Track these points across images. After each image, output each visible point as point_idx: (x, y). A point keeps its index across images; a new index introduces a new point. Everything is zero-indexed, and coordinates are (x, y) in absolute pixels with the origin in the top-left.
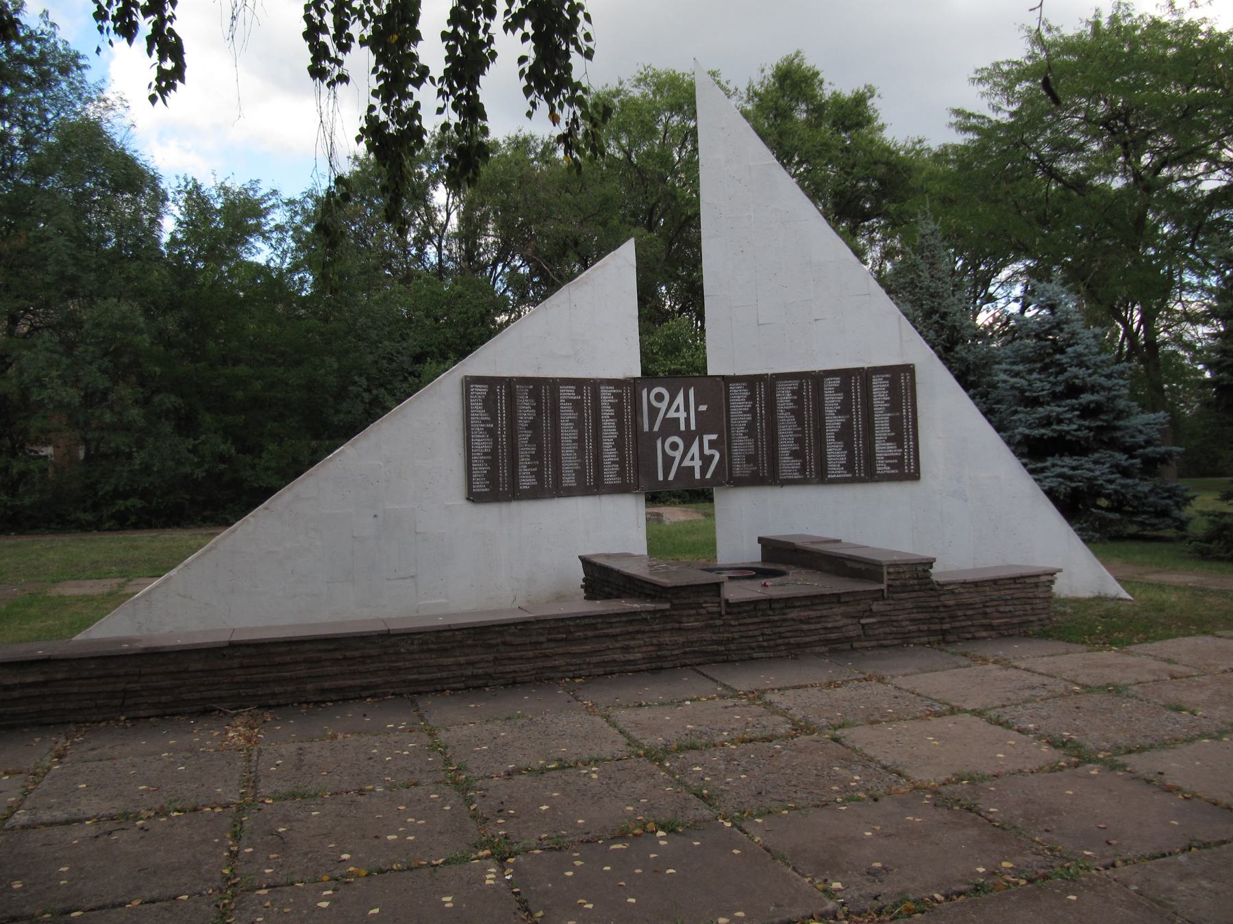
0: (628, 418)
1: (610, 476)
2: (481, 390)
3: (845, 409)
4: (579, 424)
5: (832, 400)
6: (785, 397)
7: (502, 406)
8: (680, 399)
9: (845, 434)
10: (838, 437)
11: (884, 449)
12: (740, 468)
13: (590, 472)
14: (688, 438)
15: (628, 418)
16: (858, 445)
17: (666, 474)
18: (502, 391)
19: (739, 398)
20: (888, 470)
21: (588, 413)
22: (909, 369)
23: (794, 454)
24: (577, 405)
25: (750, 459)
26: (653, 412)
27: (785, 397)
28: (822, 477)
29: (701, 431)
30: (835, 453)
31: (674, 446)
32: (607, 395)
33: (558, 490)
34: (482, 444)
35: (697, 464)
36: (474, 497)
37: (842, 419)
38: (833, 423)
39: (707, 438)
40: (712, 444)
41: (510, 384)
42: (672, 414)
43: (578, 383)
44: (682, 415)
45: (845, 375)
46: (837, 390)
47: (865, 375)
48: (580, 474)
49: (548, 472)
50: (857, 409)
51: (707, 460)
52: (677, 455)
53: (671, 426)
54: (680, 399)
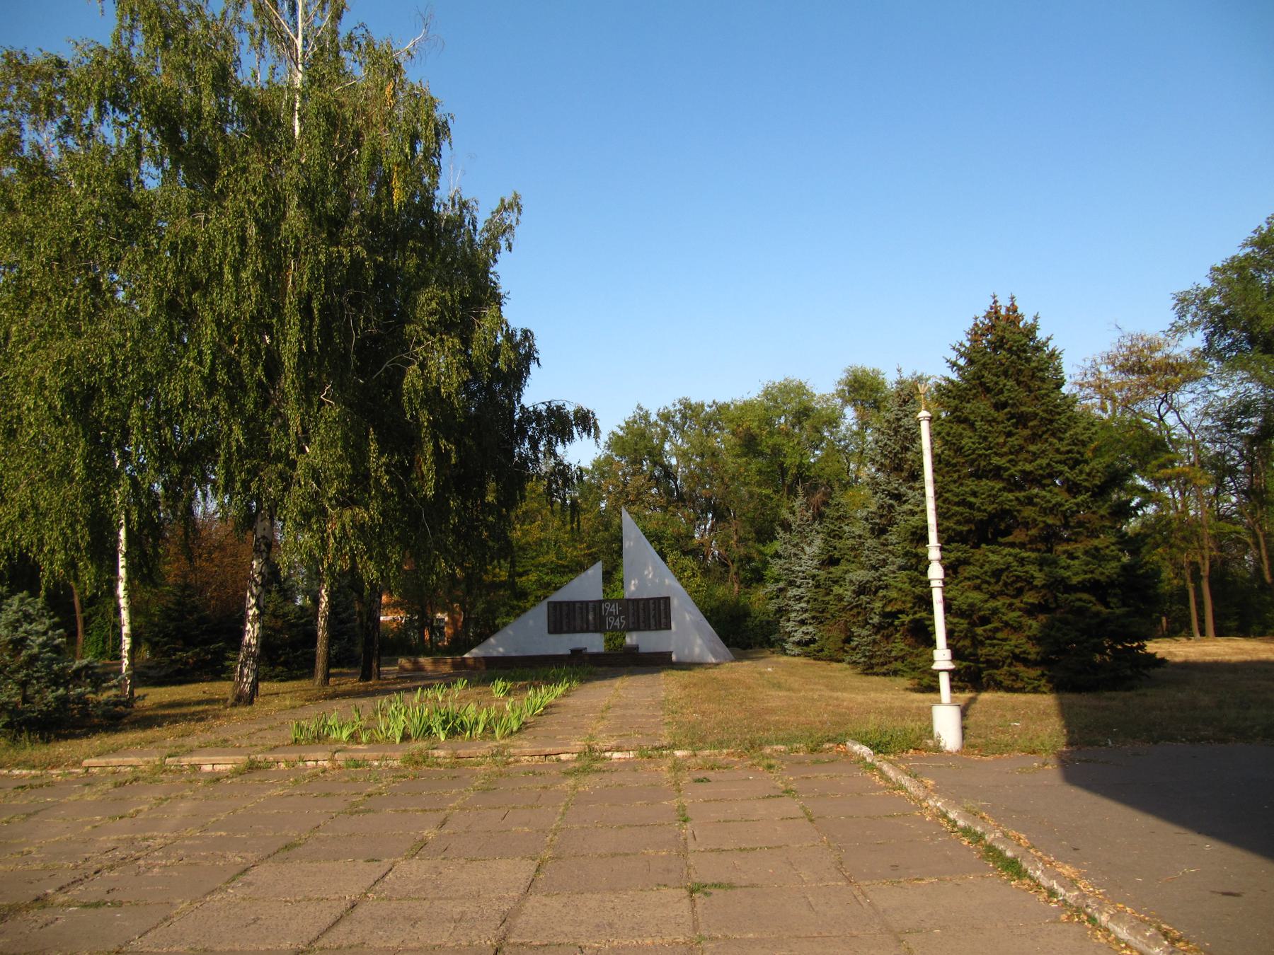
0: (597, 611)
5: (652, 606)
9: (654, 616)
11: (663, 621)
13: (585, 626)
14: (616, 617)
15: (597, 611)
22: (667, 600)
24: (581, 609)
26: (605, 610)
27: (641, 606)
32: (591, 605)
36: (550, 632)
38: (652, 613)
41: (561, 603)
47: (659, 599)
51: (621, 623)
53: (611, 614)
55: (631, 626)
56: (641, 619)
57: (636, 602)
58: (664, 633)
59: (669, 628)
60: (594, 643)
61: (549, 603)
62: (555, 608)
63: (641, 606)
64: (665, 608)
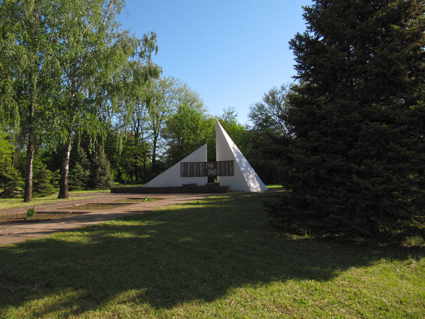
2: (183, 164)
3: (227, 166)
4: (197, 168)
7: (186, 166)
8: (211, 165)
11: (231, 171)
14: (212, 170)
17: (209, 174)
18: (186, 164)
19: (218, 165)
21: (198, 167)
23: (223, 172)
24: (196, 166)
25: (219, 172)
26: (208, 166)
27: (222, 164)
29: (214, 168)
31: (210, 171)
32: (201, 164)
33: (193, 176)
34: (183, 170)
35: (213, 173)
36: (182, 176)
40: (215, 170)
41: (187, 163)
43: (197, 163)
45: (228, 161)
48: (196, 174)
49: (192, 174)
51: (215, 173)
52: (211, 172)
53: (210, 168)
54: (211, 165)
55: (219, 174)
56: (223, 171)
57: (220, 162)
58: (231, 177)
59: (233, 175)
60: (202, 181)
61: (181, 163)
62: (185, 165)
63: (222, 164)
64: (232, 166)
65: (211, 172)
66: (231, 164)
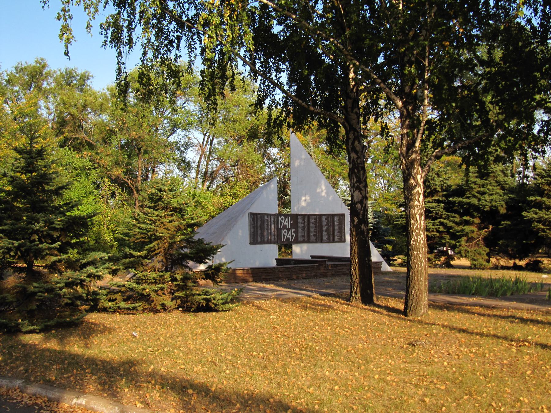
1: (273, 240)
3: (327, 224)
6: (312, 220)
9: (327, 230)
10: (326, 231)
11: (337, 234)
12: (300, 238)
14: (289, 230)
16: (331, 233)
19: (300, 221)
20: (338, 240)
23: (314, 235)
25: (303, 236)
26: (281, 223)
28: (322, 241)
29: (291, 229)
30: (325, 235)
35: (290, 237)
36: (251, 243)
37: (327, 227)
38: (325, 228)
39: (293, 230)
40: (294, 232)
42: (285, 224)
44: (287, 224)
46: (326, 219)
47: (333, 215)
50: (331, 224)
51: (292, 236)
52: (286, 234)
53: (285, 227)
57: (307, 217)
65: (286, 234)
66: (336, 222)
